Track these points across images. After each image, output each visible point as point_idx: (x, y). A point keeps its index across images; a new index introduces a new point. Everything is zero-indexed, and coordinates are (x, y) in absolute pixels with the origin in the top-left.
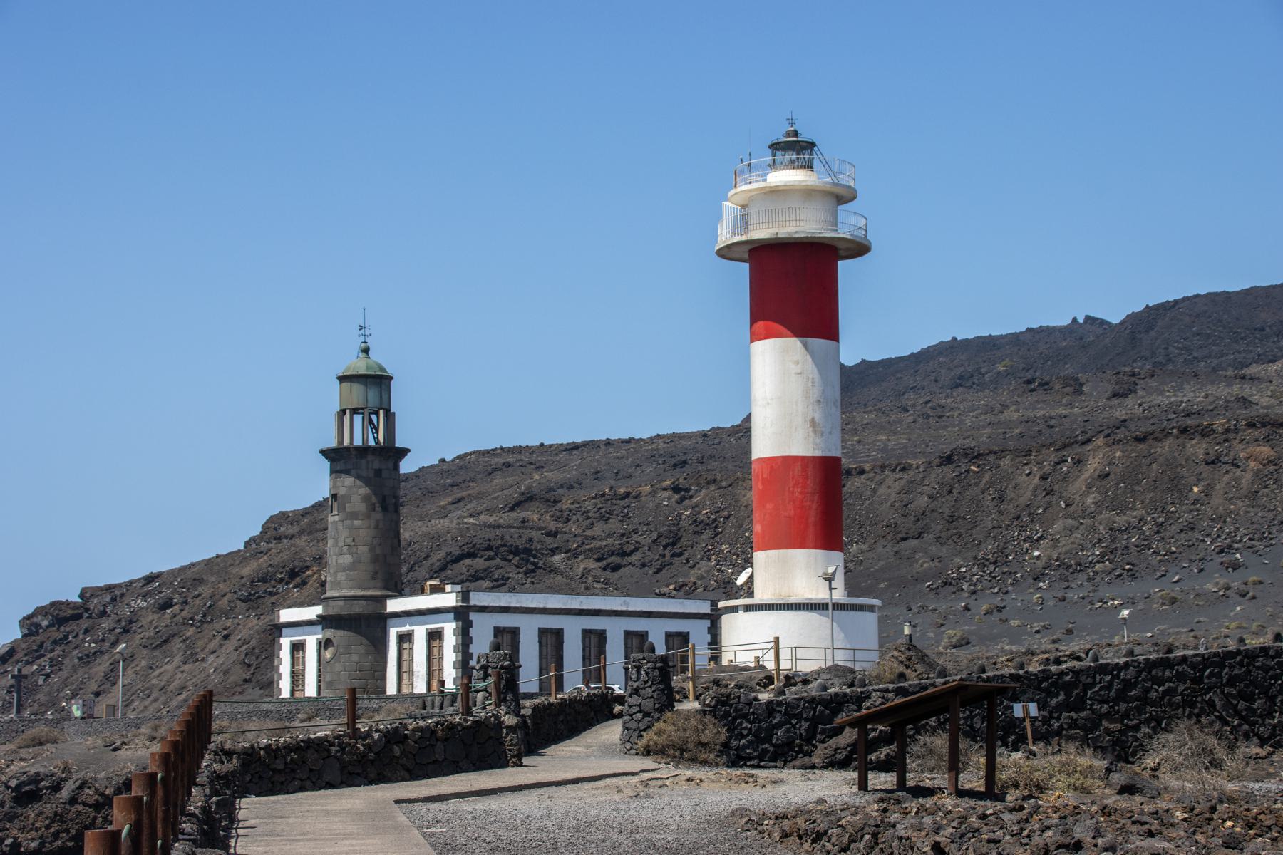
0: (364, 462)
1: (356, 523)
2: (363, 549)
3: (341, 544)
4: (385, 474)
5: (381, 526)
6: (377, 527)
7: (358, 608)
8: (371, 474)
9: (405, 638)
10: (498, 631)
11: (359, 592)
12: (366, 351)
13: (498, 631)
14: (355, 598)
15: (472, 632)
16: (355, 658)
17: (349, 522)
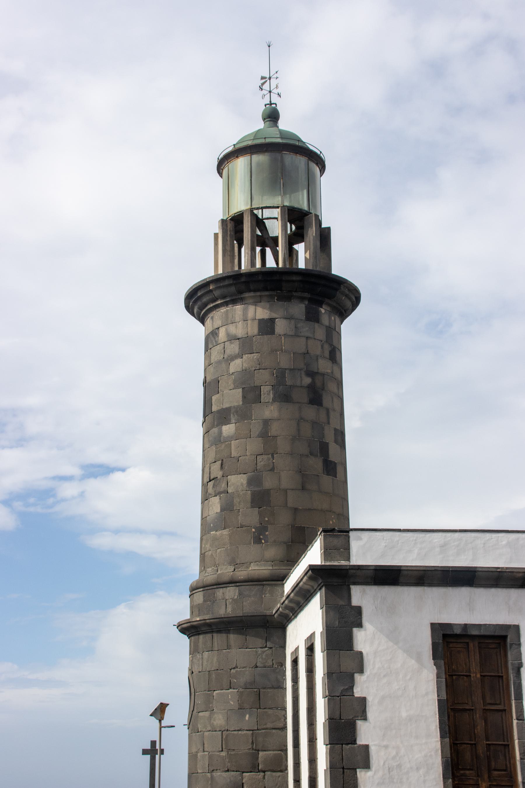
0: (238, 308)
1: (228, 429)
2: (238, 482)
3: (206, 479)
4: (281, 327)
5: (275, 429)
6: (264, 435)
7: (228, 603)
8: (253, 329)
9: (295, 662)
10: (449, 642)
11: (227, 571)
12: (272, 116)
13: (449, 642)
14: (219, 584)
15: (364, 640)
16: (219, 720)
17: (215, 430)
